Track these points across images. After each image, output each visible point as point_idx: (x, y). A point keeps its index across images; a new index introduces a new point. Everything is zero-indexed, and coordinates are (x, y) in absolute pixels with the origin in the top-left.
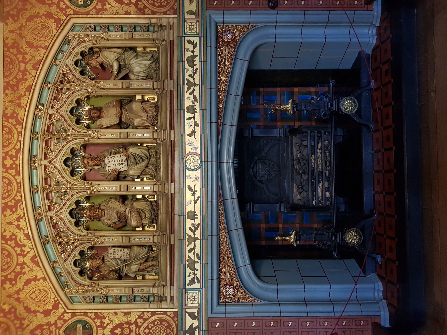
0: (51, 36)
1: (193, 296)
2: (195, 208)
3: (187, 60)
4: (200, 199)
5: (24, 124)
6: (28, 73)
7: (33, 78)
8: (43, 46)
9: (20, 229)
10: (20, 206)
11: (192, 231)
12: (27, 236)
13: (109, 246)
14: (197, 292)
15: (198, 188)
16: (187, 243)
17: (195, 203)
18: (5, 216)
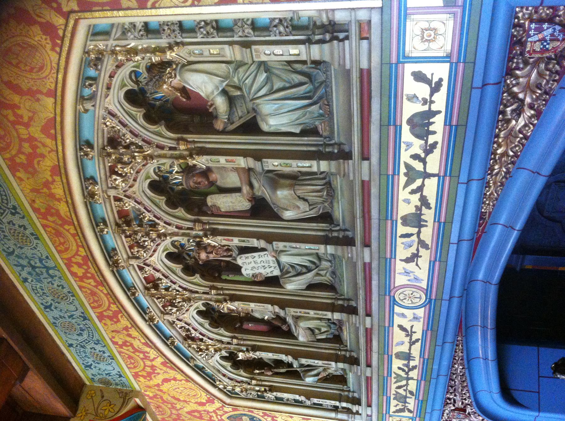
0: (51, 68)
2: (410, 349)
3: (410, 121)
5: (76, 223)
6: (39, 145)
7: (54, 153)
8: (45, 91)
9: (134, 338)
10: (122, 317)
11: (404, 370)
12: (146, 344)
15: (419, 328)
16: (394, 380)
17: (411, 345)
18: (105, 324)
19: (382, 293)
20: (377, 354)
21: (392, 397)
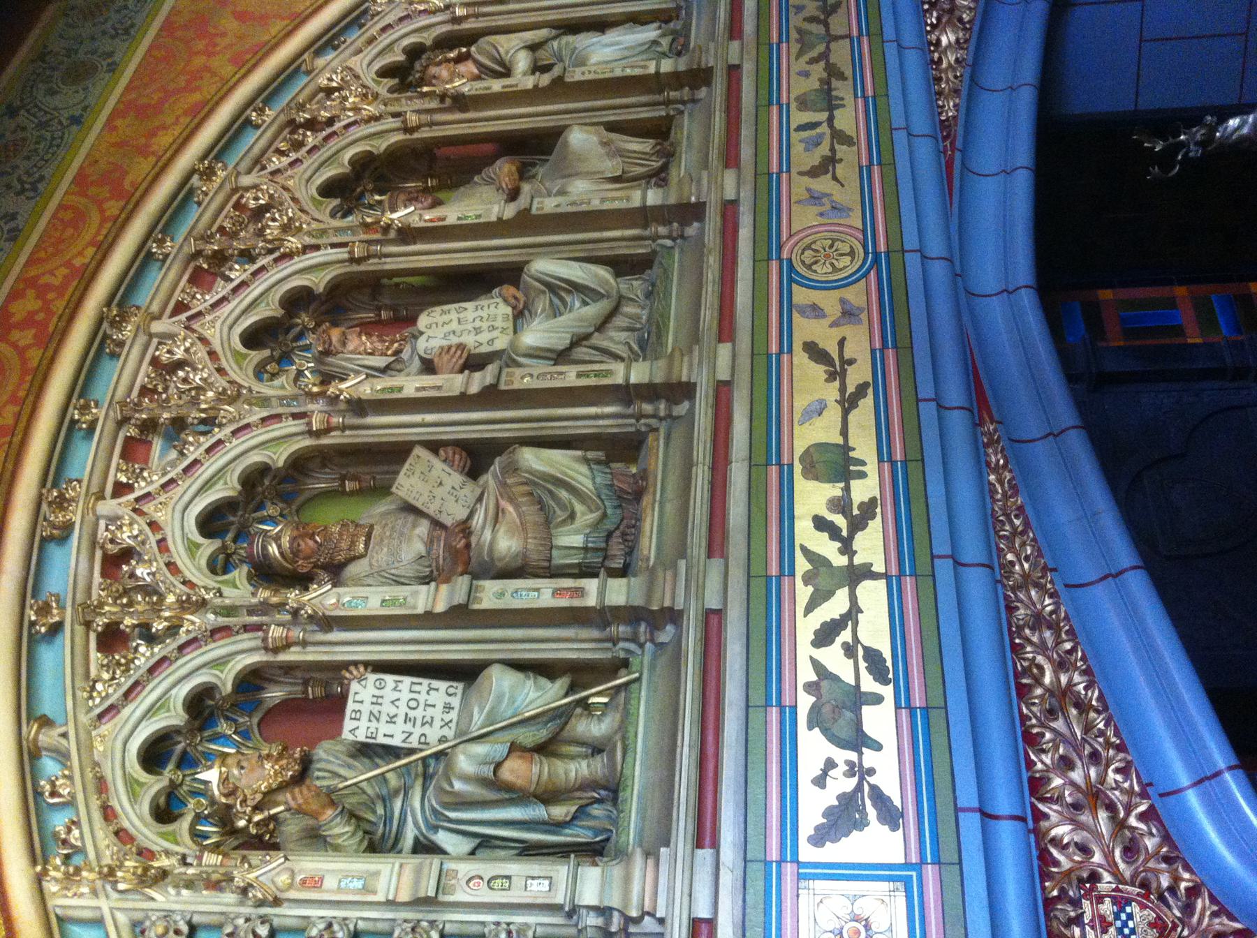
1: (856, 919)
2: (844, 432)
4: (870, 391)
11: (834, 532)
13: (356, 663)
14: (885, 886)
15: (859, 344)
16: (804, 593)
19: (762, 255)
20: (746, 464)
21: (805, 702)
